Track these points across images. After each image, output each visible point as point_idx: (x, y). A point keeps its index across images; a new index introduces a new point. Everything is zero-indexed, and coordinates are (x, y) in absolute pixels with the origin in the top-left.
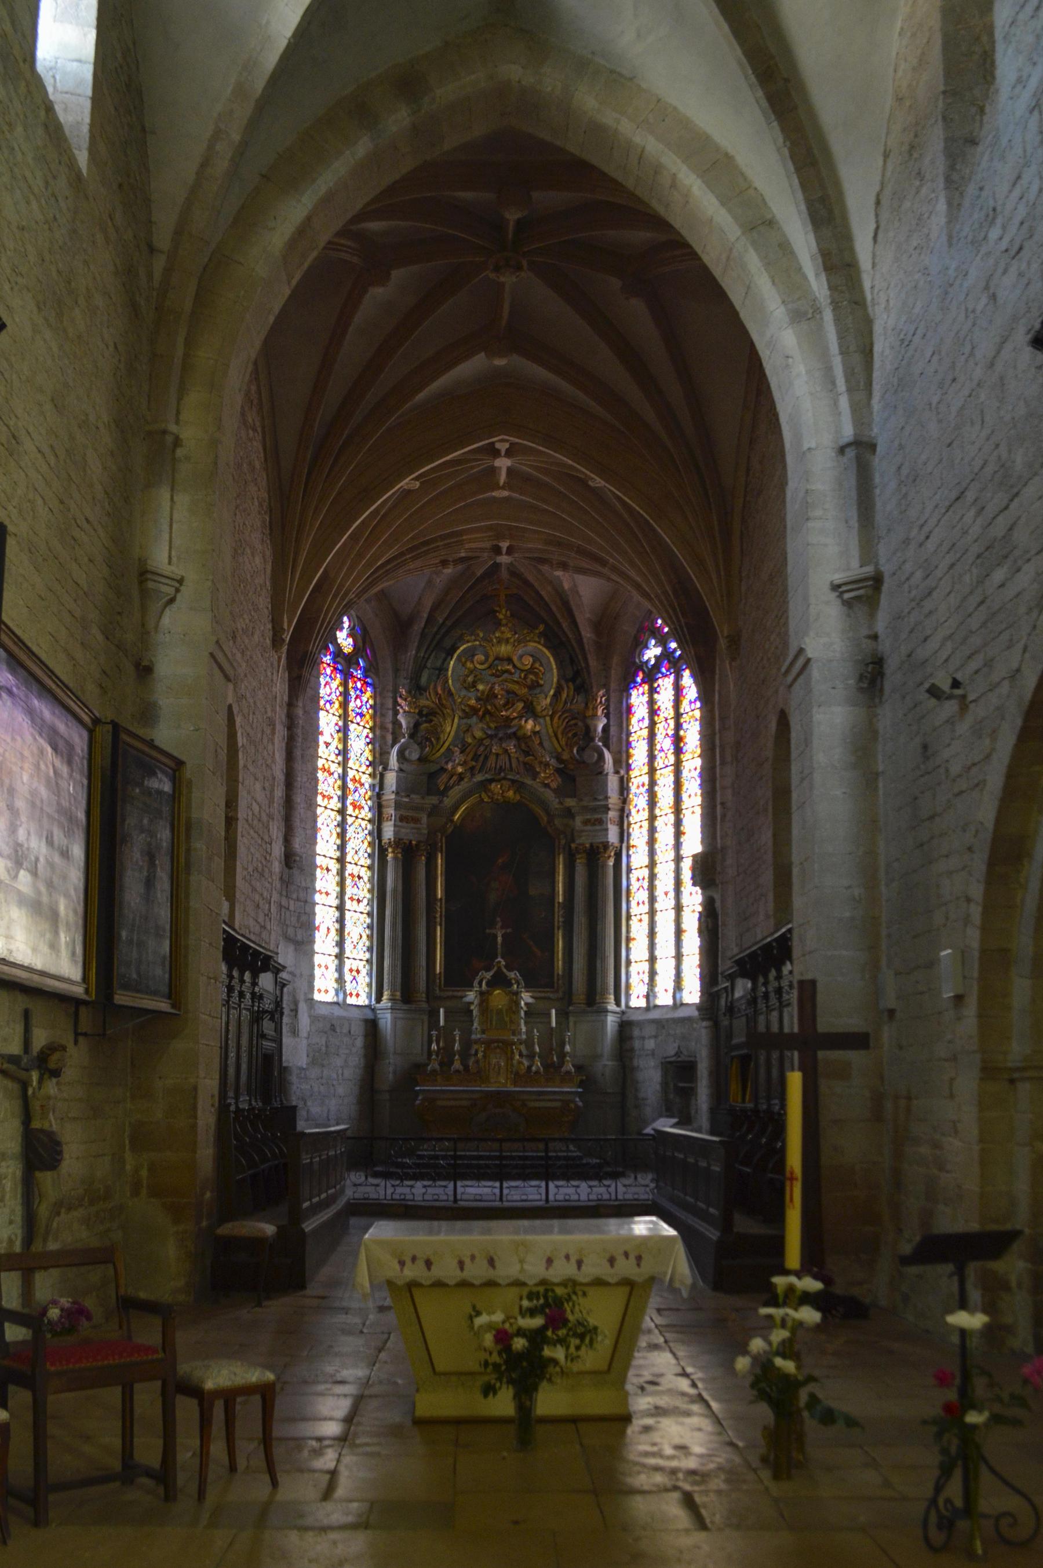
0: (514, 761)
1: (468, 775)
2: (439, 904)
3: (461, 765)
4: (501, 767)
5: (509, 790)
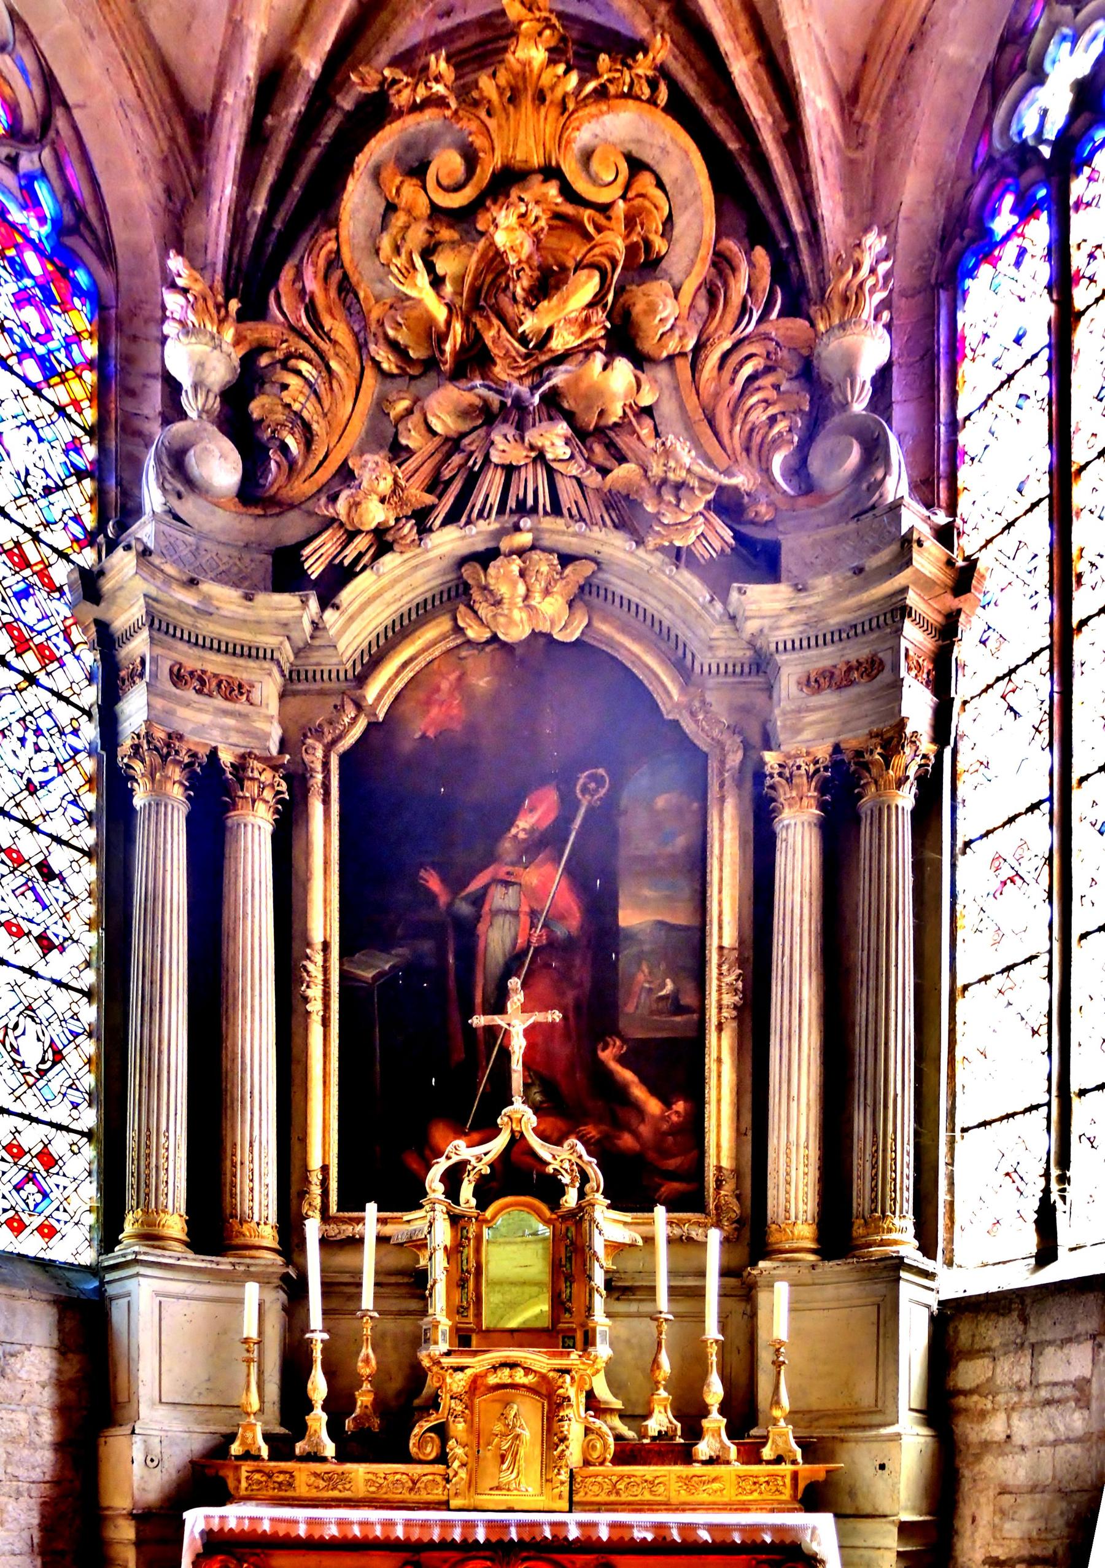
0: (568, 492)
1: (408, 528)
2: (319, 958)
3: (382, 500)
4: (521, 503)
5: (547, 592)
